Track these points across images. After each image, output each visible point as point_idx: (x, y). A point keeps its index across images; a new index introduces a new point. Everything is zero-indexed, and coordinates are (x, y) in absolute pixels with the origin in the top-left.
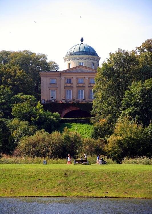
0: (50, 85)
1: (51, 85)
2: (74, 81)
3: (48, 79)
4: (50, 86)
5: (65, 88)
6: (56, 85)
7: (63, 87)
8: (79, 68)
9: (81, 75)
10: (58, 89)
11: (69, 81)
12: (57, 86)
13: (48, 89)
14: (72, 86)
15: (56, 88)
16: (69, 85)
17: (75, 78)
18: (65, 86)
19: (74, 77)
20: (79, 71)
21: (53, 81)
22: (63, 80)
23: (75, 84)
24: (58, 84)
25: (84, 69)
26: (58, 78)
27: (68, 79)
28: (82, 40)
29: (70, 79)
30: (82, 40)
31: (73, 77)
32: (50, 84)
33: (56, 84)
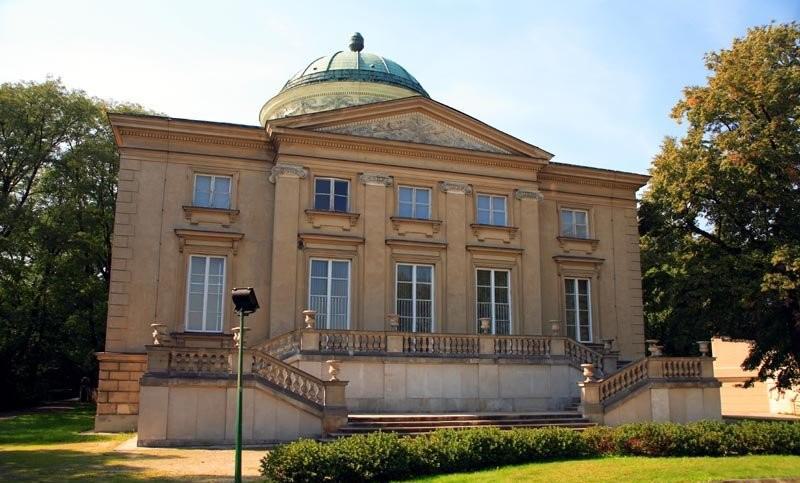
0: (188, 217)
1: (196, 217)
2: (371, 199)
3: (177, 170)
4: (186, 225)
5: (301, 245)
7: (285, 234)
8: (407, 118)
9: (419, 163)
10: (249, 250)
11: (332, 198)
12: (243, 226)
13: (171, 245)
14: (356, 231)
15: (236, 240)
16: (334, 224)
17: (379, 179)
18: (307, 227)
19: (369, 172)
20: (407, 134)
21: (214, 191)
22: (292, 188)
23: (375, 226)
24: (245, 213)
25: (438, 126)
26: (250, 174)
27: (323, 185)
28: (358, 44)
29: (341, 187)
31: (361, 168)
32: (189, 210)
33: (234, 214)
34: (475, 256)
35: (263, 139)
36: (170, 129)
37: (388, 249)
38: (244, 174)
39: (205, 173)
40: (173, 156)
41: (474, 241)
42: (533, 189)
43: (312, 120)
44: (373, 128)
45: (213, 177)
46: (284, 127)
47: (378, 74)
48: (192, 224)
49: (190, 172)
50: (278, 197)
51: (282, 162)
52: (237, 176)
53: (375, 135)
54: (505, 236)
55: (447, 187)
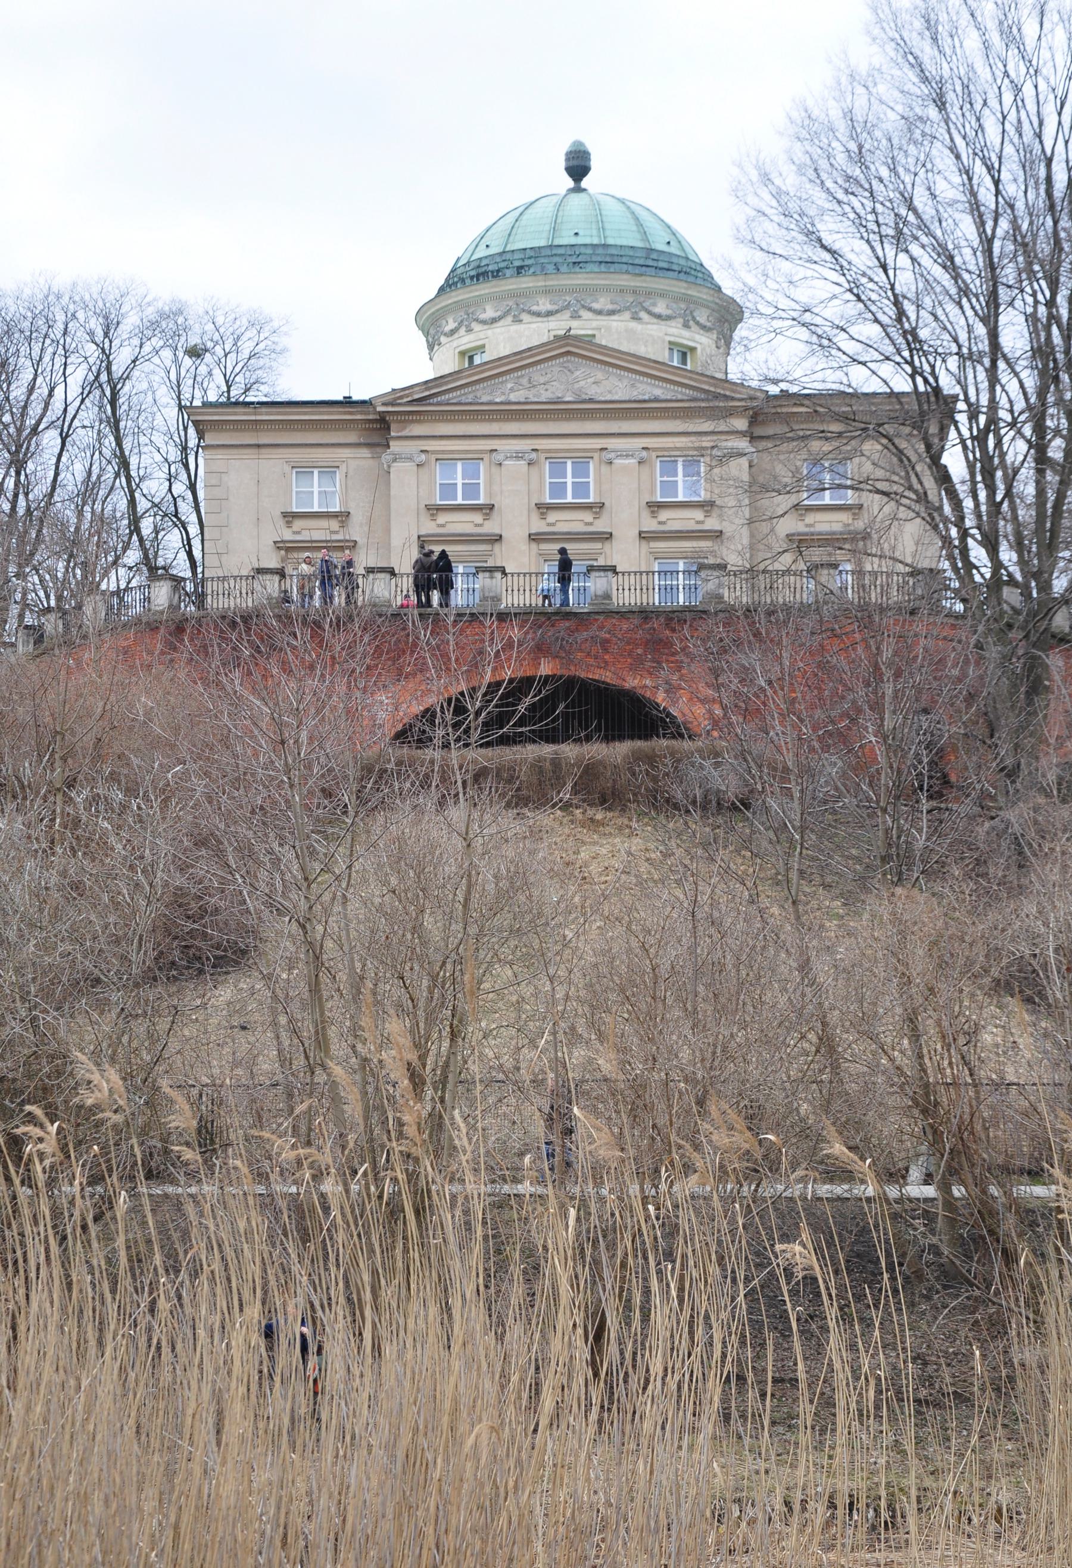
0: (289, 524)
1: (298, 524)
6: (343, 524)
17: (518, 456)
28: (578, 167)
30: (578, 167)
32: (290, 517)
34: (653, 544)
35: (371, 417)
36: (259, 418)
37: (534, 546)
38: (353, 464)
39: (303, 470)
40: (263, 451)
41: (650, 525)
42: (743, 444)
43: (427, 389)
44: (509, 386)
45: (316, 472)
46: (392, 404)
47: (583, 250)
48: (295, 533)
49: (287, 468)
50: (392, 493)
51: (395, 446)
52: (343, 468)
53: (513, 397)
54: (698, 514)
55: (612, 455)
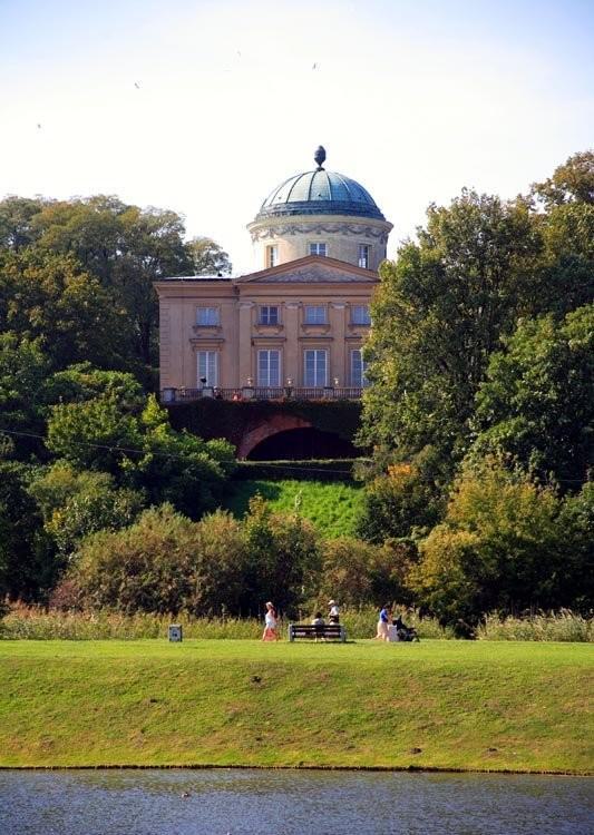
0: (196, 332)
1: (200, 331)
2: (290, 316)
3: (189, 307)
4: (195, 336)
5: (253, 344)
6: (219, 332)
7: (245, 339)
8: (309, 266)
9: (318, 292)
10: (228, 347)
11: (270, 317)
12: (224, 335)
13: (188, 348)
14: (282, 334)
15: (220, 342)
16: (270, 331)
17: (294, 304)
18: (256, 334)
19: (289, 300)
20: (310, 276)
21: (209, 316)
22: (247, 313)
23: (292, 328)
24: (225, 327)
25: (328, 269)
26: (226, 305)
27: (265, 310)
28: (321, 156)
29: (274, 310)
30: (321, 156)
31: (284, 299)
32: (197, 327)
33: (218, 328)
